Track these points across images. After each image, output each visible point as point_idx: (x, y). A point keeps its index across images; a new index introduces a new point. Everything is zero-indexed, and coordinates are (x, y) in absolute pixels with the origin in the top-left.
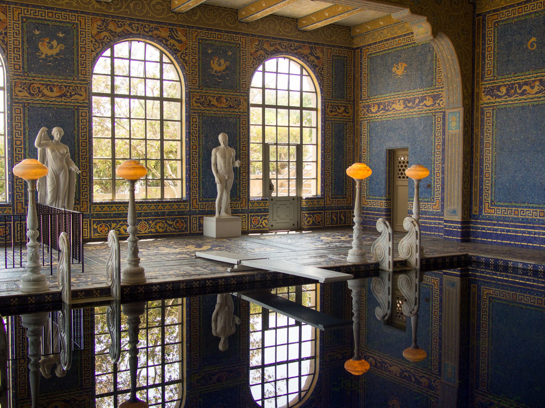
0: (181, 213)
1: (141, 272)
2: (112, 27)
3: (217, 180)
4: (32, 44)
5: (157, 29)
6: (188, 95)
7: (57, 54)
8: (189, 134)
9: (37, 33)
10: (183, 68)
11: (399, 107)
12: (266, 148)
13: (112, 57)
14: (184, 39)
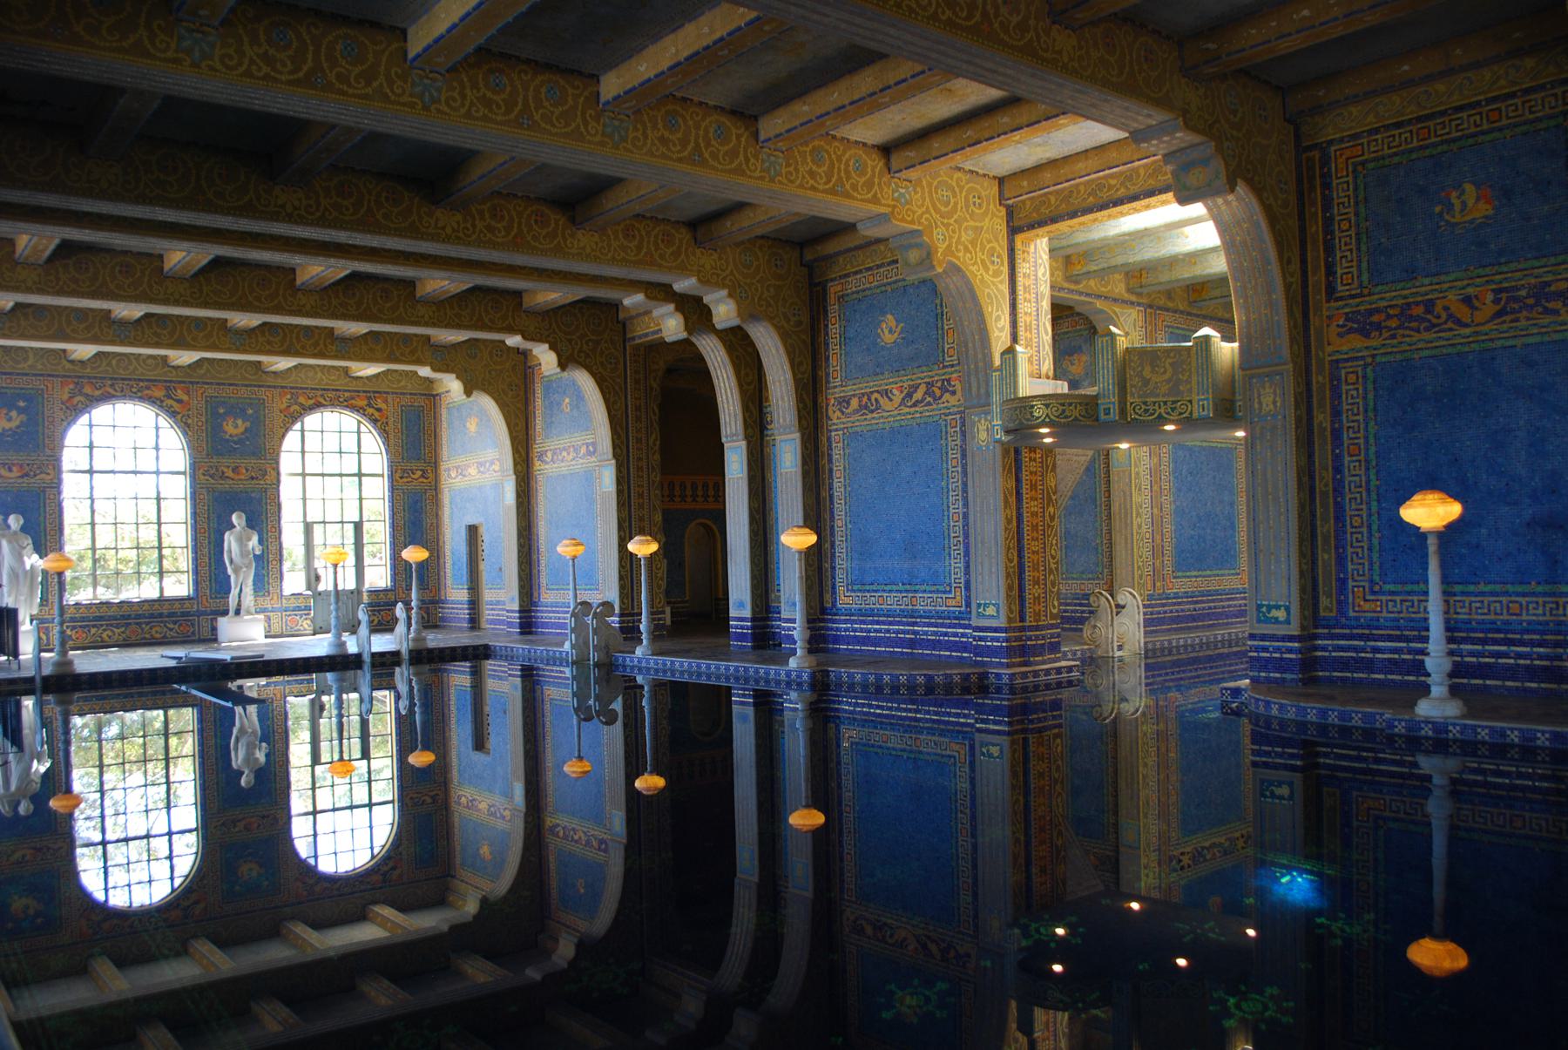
0: (188, 614)
2: (88, 390)
3: (230, 571)
5: (148, 388)
6: (195, 466)
8: (195, 514)
10: (185, 434)
11: (473, 471)
12: (308, 528)
13: (91, 426)
14: (185, 398)
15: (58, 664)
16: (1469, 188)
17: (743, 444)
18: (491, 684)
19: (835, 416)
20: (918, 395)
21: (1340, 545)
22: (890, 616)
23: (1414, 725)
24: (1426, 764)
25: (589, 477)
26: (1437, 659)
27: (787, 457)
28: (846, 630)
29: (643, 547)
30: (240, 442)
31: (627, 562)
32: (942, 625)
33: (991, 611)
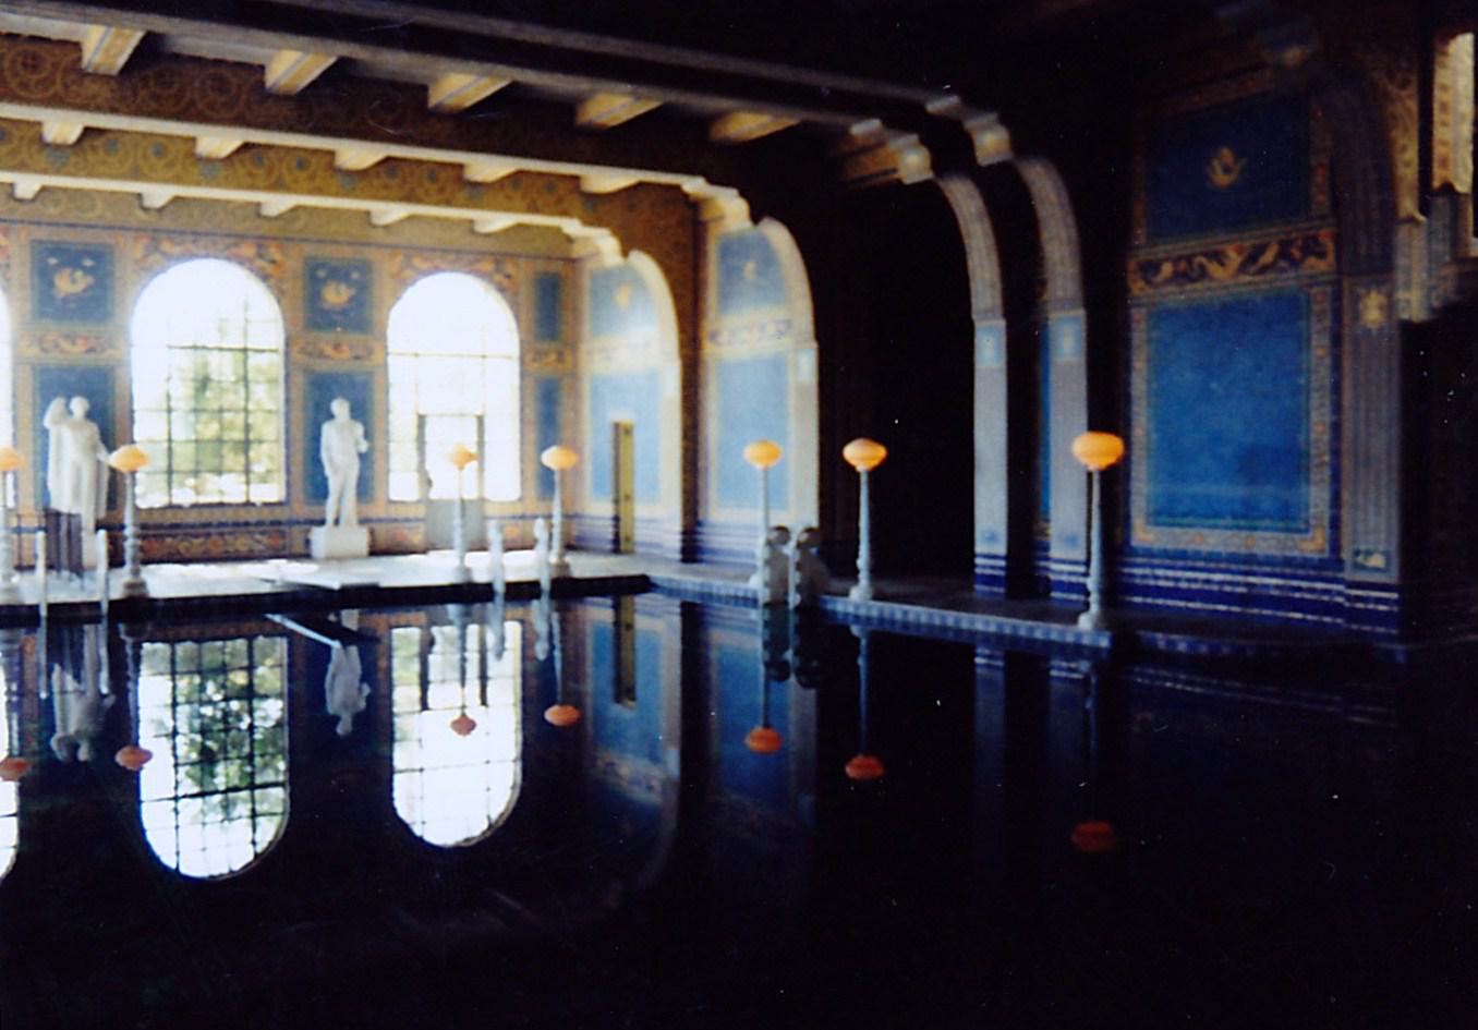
1: (143, 585)
2: (166, 246)
4: (44, 277)
5: (236, 245)
7: (85, 291)
9: (53, 261)
15: (130, 586)
17: (1001, 323)
18: (642, 623)
19: (1138, 287)
20: (1268, 257)
22: (1212, 560)
25: (778, 365)
27: (1067, 343)
28: (1144, 577)
29: (861, 455)
30: (344, 312)
31: (834, 478)
32: (1294, 577)
33: (1377, 561)
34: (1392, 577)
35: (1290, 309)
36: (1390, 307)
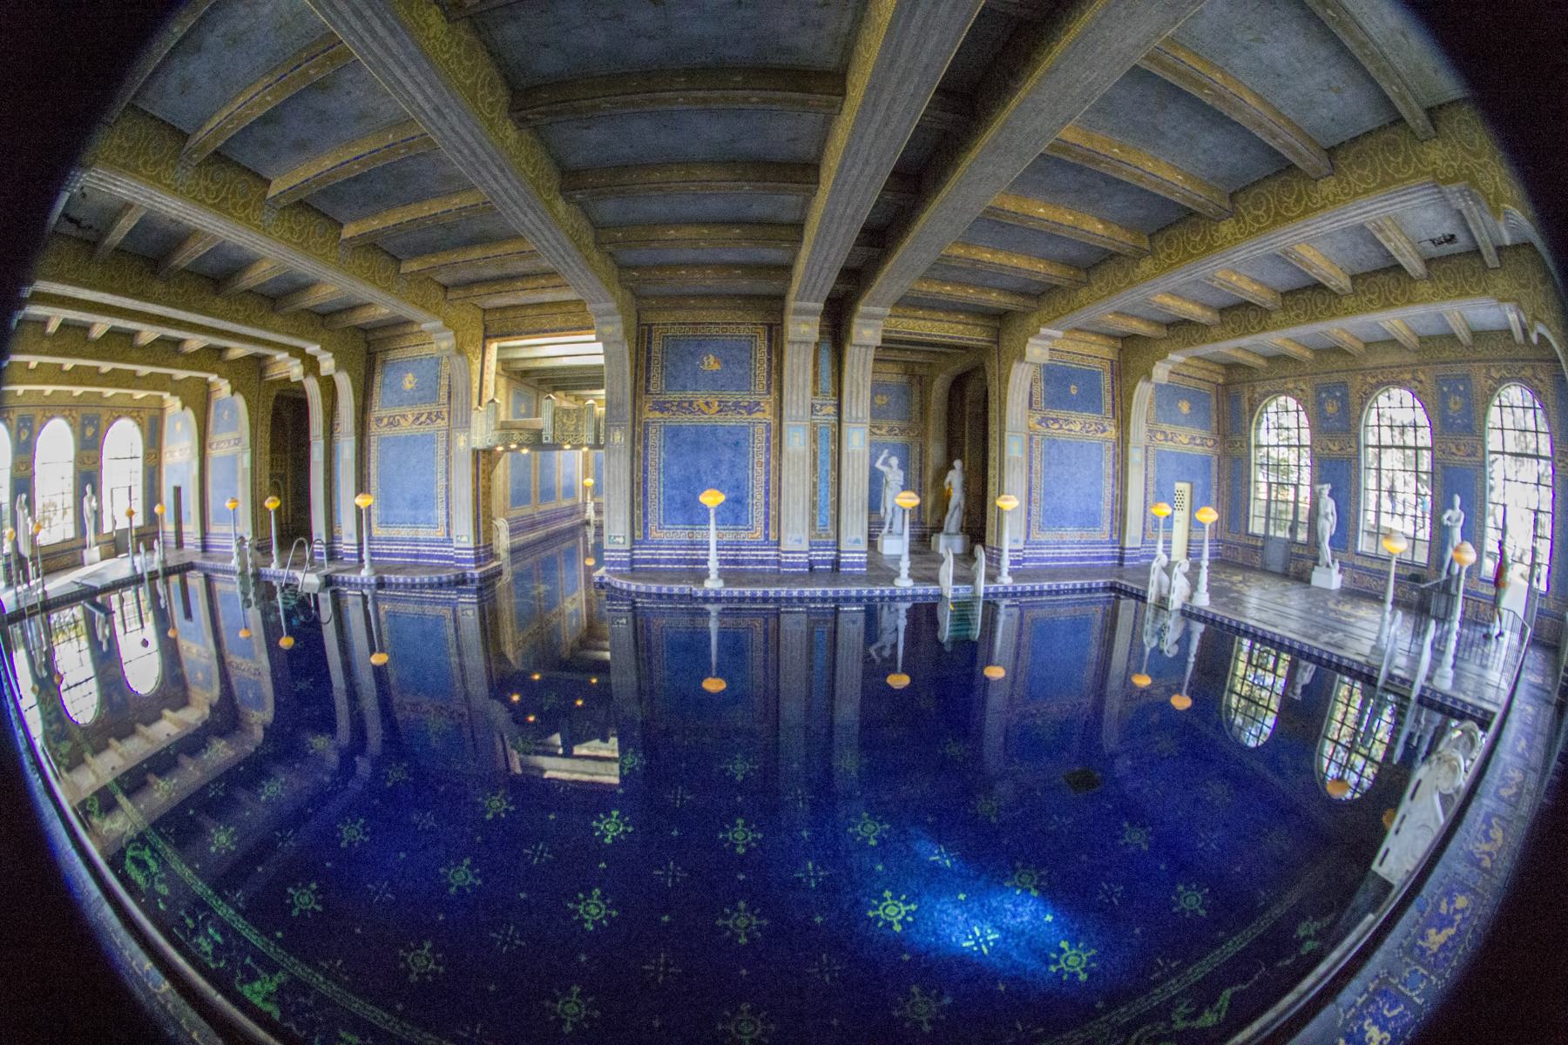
16: (712, 358)
20: (423, 419)
21: (645, 507)
23: (706, 592)
24: (708, 607)
26: (713, 565)
34: (471, 545)
35: (430, 440)
36: (468, 442)
